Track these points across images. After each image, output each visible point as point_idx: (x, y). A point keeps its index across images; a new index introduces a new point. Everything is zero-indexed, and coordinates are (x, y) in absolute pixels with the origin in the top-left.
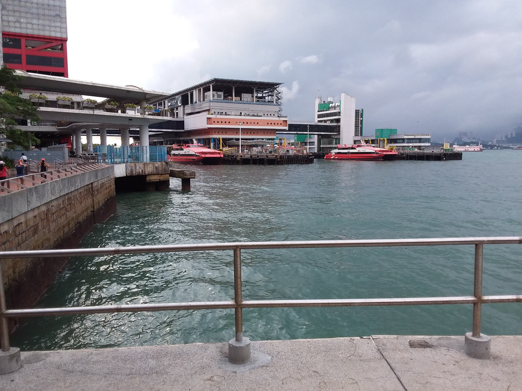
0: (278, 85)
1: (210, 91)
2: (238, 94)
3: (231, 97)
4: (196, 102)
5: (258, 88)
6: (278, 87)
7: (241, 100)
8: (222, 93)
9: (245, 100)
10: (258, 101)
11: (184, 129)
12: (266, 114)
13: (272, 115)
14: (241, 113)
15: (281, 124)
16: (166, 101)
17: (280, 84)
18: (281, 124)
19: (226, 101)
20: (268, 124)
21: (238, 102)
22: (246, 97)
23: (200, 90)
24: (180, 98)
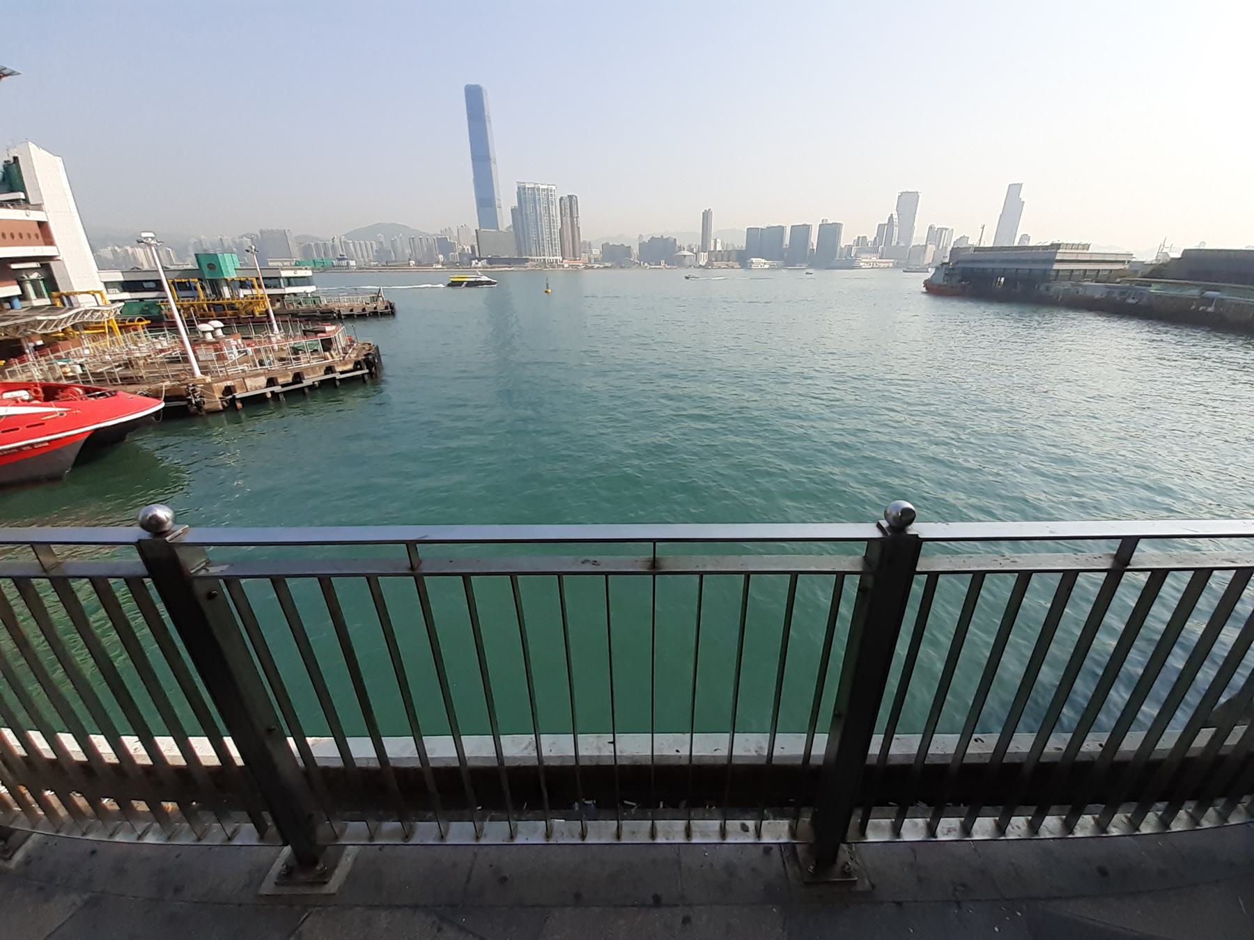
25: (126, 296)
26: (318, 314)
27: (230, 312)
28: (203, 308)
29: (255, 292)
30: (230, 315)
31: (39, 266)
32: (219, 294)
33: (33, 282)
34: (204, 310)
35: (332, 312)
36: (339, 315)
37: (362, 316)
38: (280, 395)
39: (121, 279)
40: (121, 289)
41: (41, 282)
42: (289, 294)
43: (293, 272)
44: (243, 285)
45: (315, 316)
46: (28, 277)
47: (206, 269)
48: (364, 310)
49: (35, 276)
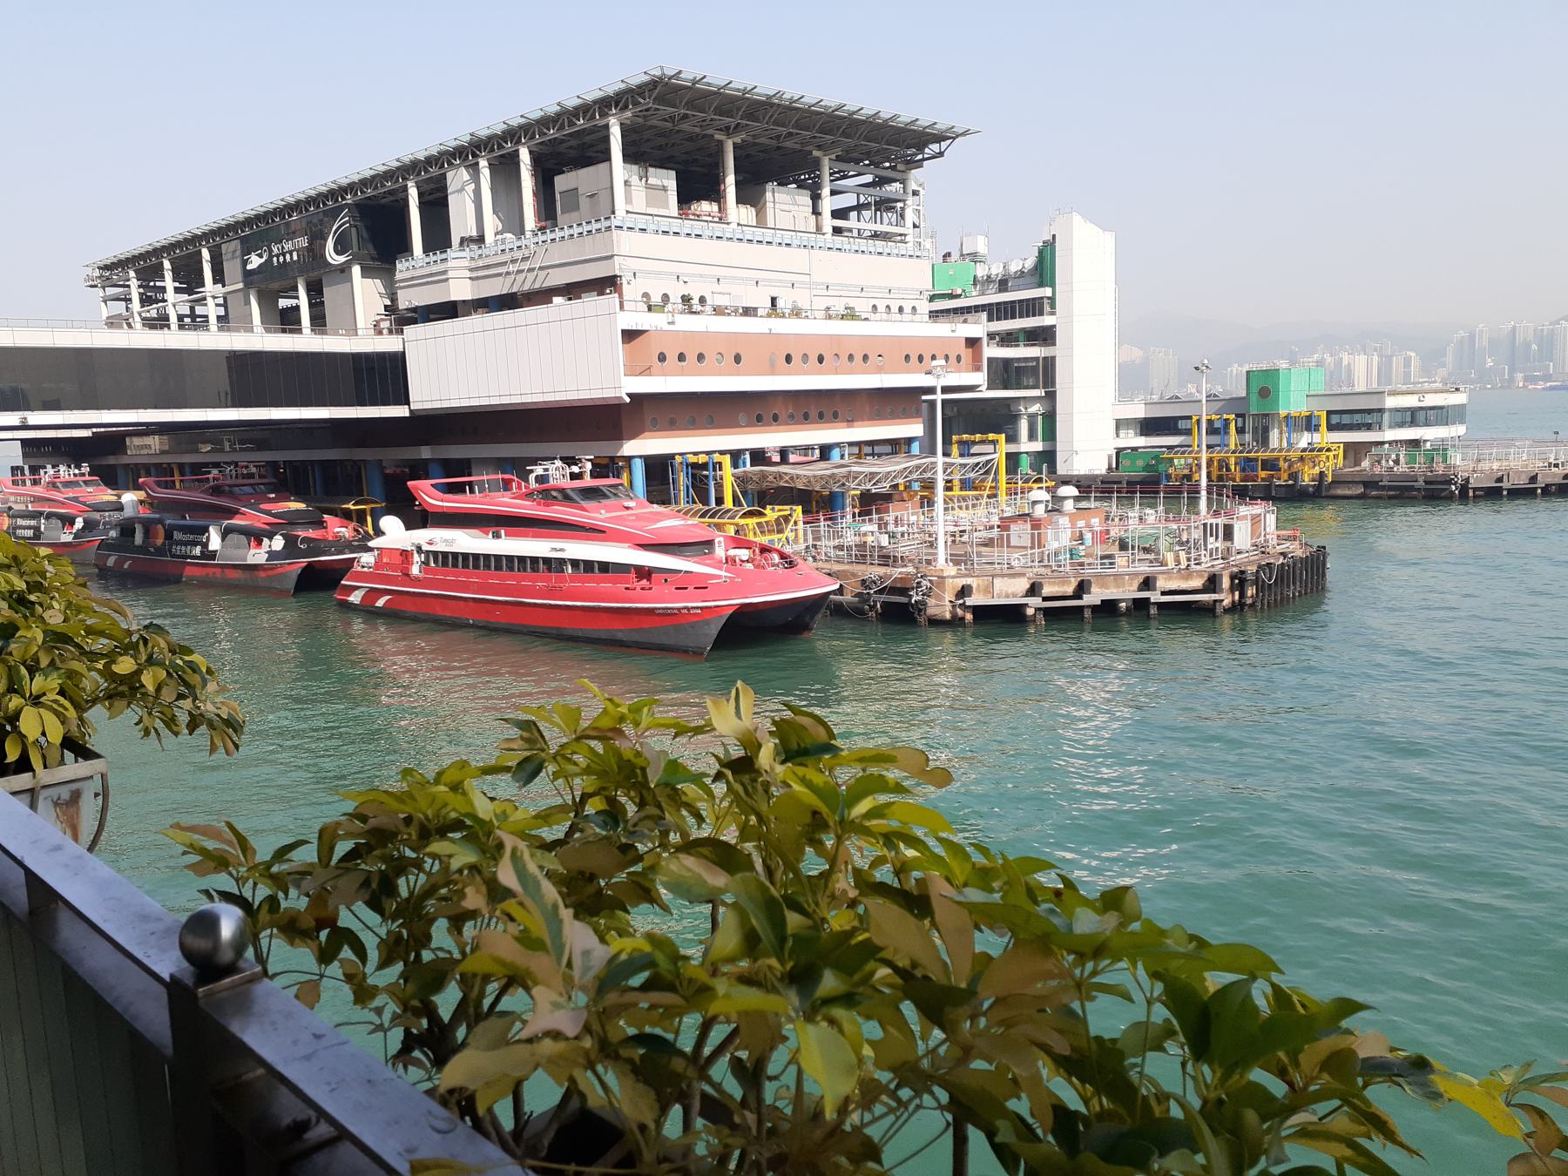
0: (938, 141)
1: (606, 156)
2: (750, 194)
3: (715, 207)
4: (480, 239)
5: (839, 159)
6: (941, 154)
7: (761, 222)
8: (669, 180)
9: (784, 221)
10: (837, 231)
11: (408, 403)
12: (881, 308)
13: (907, 309)
14: (773, 300)
15: (959, 359)
16: (230, 248)
17: (939, 138)
18: (959, 359)
19: (688, 226)
20: (907, 358)
21: (748, 233)
22: (786, 203)
23: (505, 168)
24: (342, 222)
25: (1141, 441)
26: (1421, 483)
27: (1263, 474)
28: (1227, 465)
29: (1317, 437)
30: (1263, 479)
31: (1043, 394)
32: (1264, 440)
33: (1032, 417)
34: (1228, 469)
35: (1449, 482)
36: (1464, 489)
37: (1517, 493)
38: (1086, 610)
39: (1142, 415)
40: (1138, 431)
41: (1040, 418)
42: (1390, 443)
43: (1416, 397)
44: (1309, 424)
45: (1412, 488)
46: (1026, 409)
47: (1254, 398)
48: (1533, 479)
49: (1036, 408)
